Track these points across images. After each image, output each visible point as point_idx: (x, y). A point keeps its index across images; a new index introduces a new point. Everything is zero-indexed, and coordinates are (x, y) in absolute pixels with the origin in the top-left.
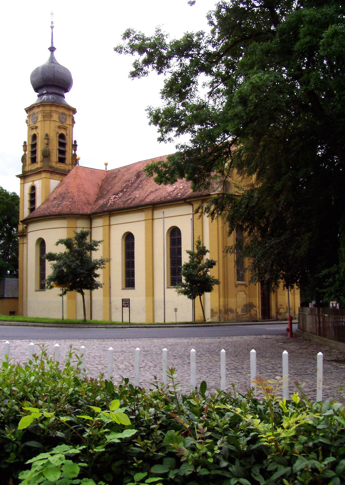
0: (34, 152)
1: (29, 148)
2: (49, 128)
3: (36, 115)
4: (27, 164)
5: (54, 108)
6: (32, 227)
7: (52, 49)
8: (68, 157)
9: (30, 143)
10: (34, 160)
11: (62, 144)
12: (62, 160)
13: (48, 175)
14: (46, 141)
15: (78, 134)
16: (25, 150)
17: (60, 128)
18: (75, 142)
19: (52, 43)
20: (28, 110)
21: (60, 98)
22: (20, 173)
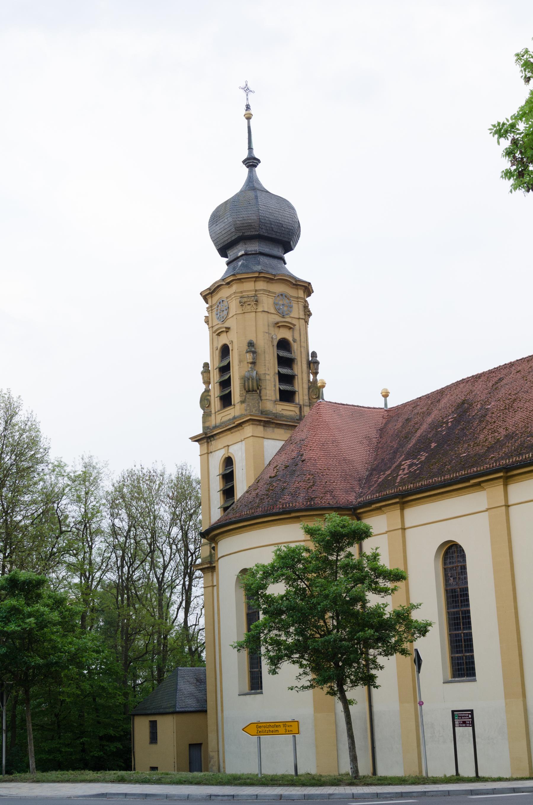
0: (225, 384)
1: (215, 377)
2: (254, 328)
3: (225, 303)
4: (213, 412)
5: (261, 285)
6: (226, 545)
7: (251, 162)
8: (300, 387)
9: (217, 364)
10: (226, 400)
11: (285, 362)
12: (287, 396)
13: (259, 430)
14: (249, 357)
15: (319, 337)
16: (207, 382)
17: (279, 327)
18: (314, 354)
19: (250, 148)
20: (208, 295)
21: (275, 262)
22: (199, 430)
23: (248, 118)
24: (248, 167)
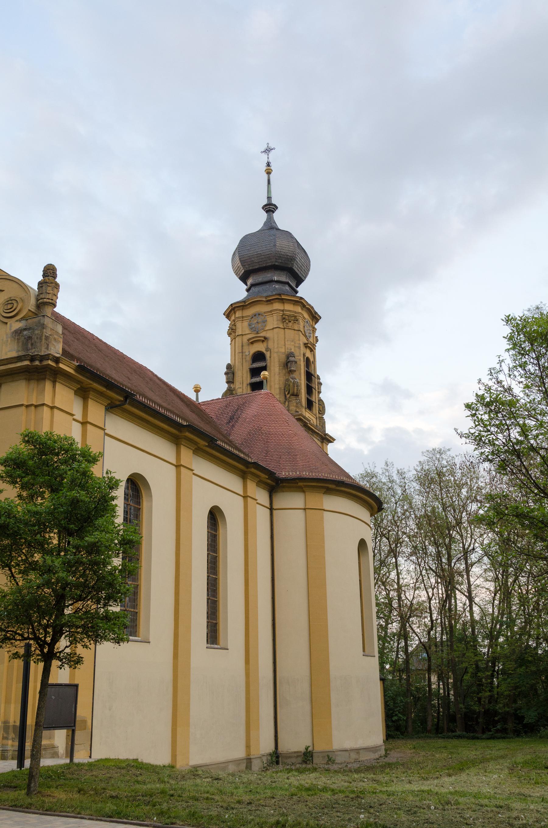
5: (299, 309)
7: (270, 208)
12: (310, 405)
23: (269, 173)
24: (267, 212)
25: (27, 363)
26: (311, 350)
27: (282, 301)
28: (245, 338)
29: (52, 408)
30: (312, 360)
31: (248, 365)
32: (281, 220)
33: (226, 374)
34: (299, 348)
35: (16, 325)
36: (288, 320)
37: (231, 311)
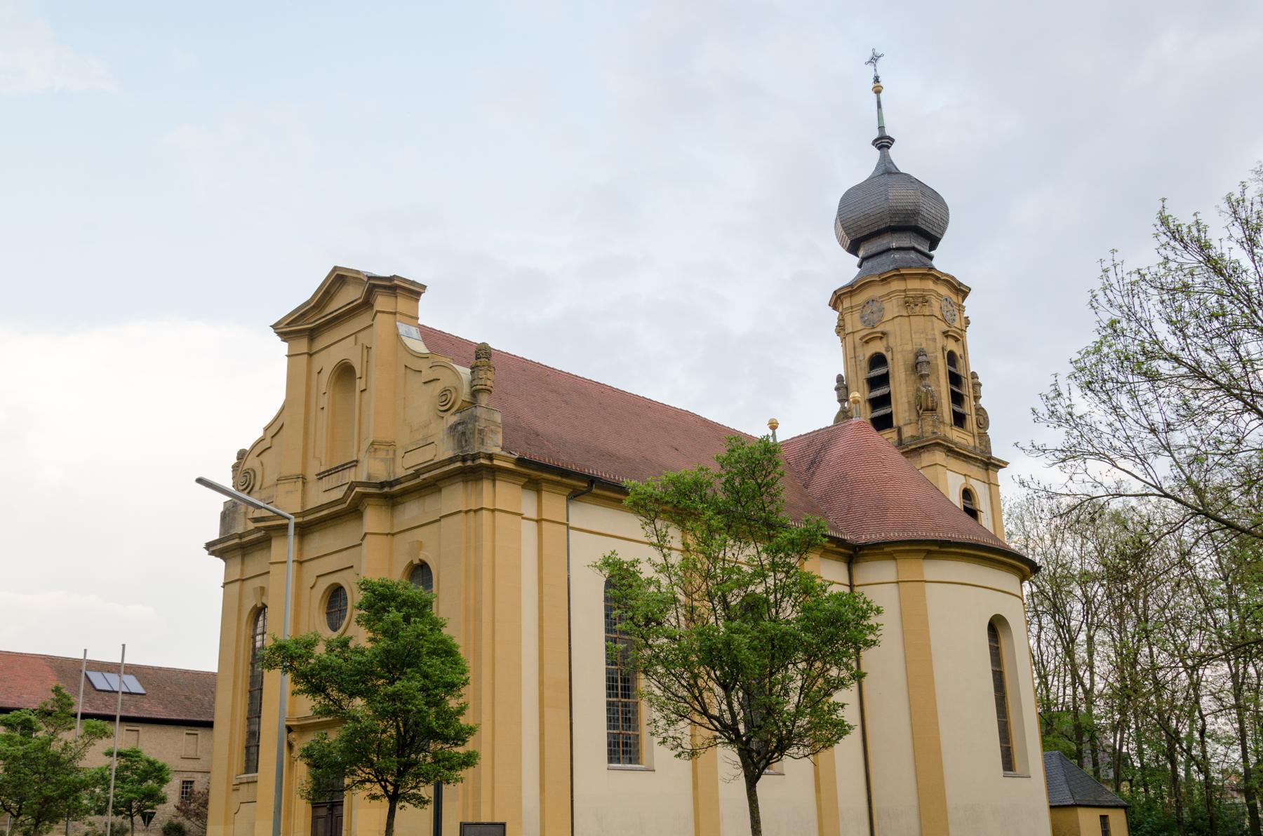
5: (929, 285)
7: (883, 143)
12: (959, 419)
19: (881, 128)
23: (878, 91)
24: (879, 148)
25: (459, 464)
26: (957, 340)
27: (903, 277)
28: (858, 336)
29: (493, 511)
30: (958, 352)
31: (864, 373)
32: (900, 157)
33: (837, 389)
34: (934, 340)
35: (452, 419)
36: (914, 303)
37: (837, 300)
